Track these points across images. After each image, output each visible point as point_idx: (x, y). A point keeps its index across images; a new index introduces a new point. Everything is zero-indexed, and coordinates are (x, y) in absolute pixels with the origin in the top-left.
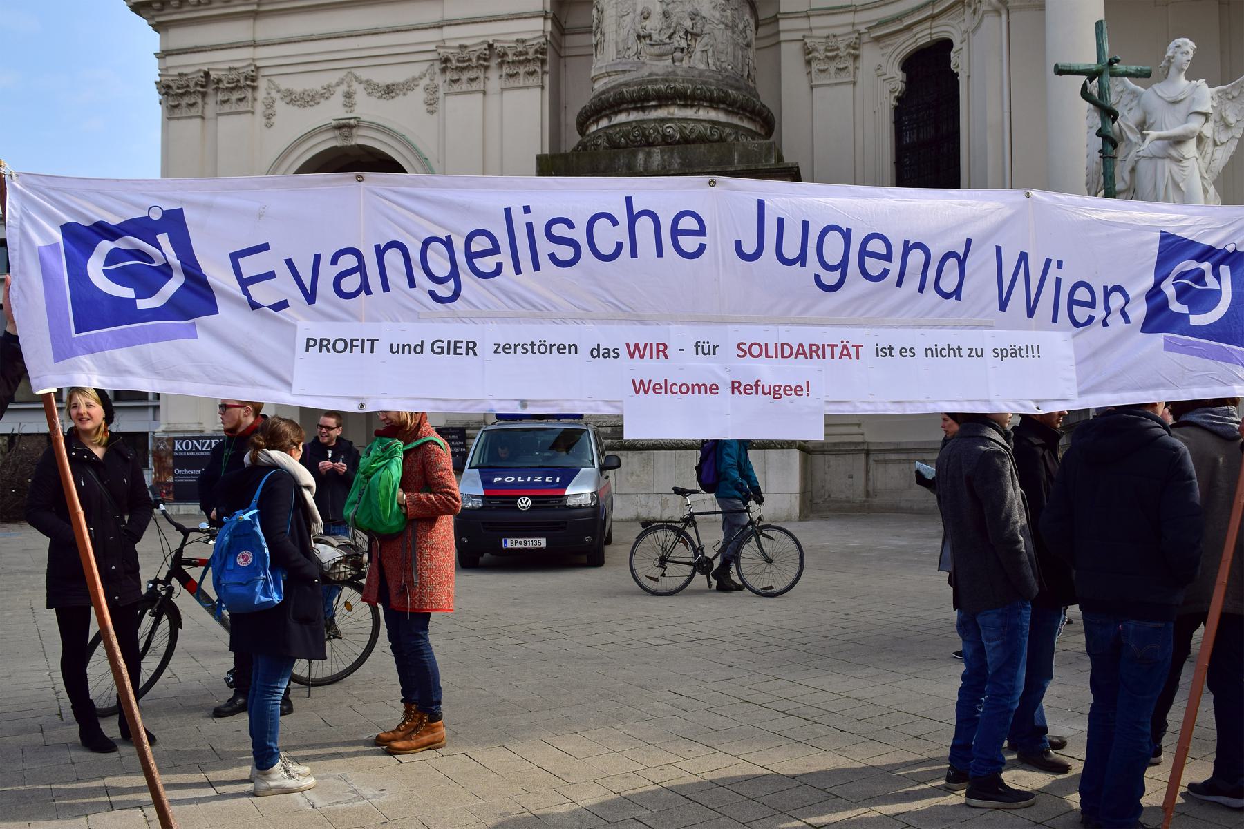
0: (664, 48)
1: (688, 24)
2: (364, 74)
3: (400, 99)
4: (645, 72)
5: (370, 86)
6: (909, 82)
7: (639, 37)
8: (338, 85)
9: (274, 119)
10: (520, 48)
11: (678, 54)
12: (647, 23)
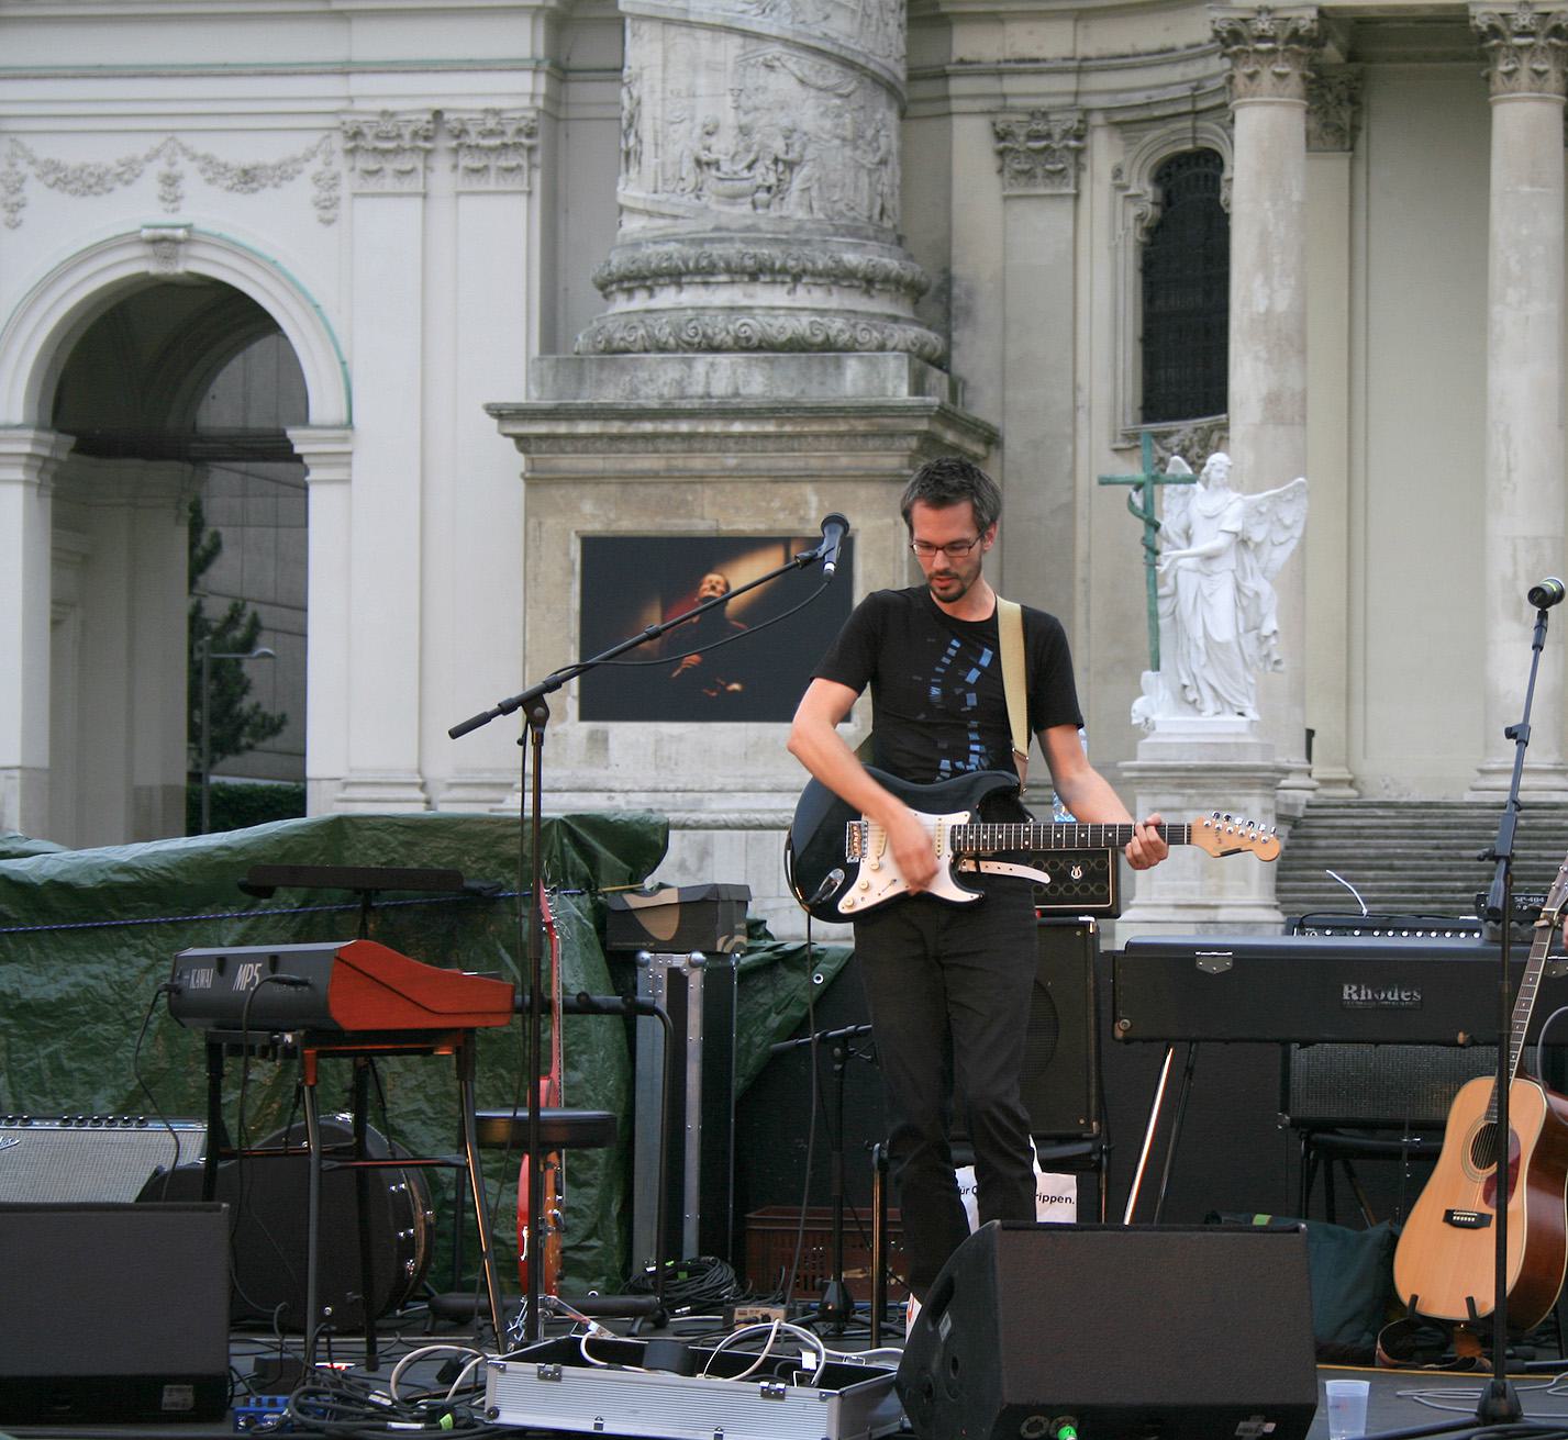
0: (740, 186)
1: (778, 146)
2: (201, 144)
3: (269, 192)
4: (705, 225)
5: (213, 169)
6: (1167, 202)
7: (699, 162)
8: (149, 159)
9: (22, 214)
10: (491, 123)
11: (762, 196)
12: (712, 141)
